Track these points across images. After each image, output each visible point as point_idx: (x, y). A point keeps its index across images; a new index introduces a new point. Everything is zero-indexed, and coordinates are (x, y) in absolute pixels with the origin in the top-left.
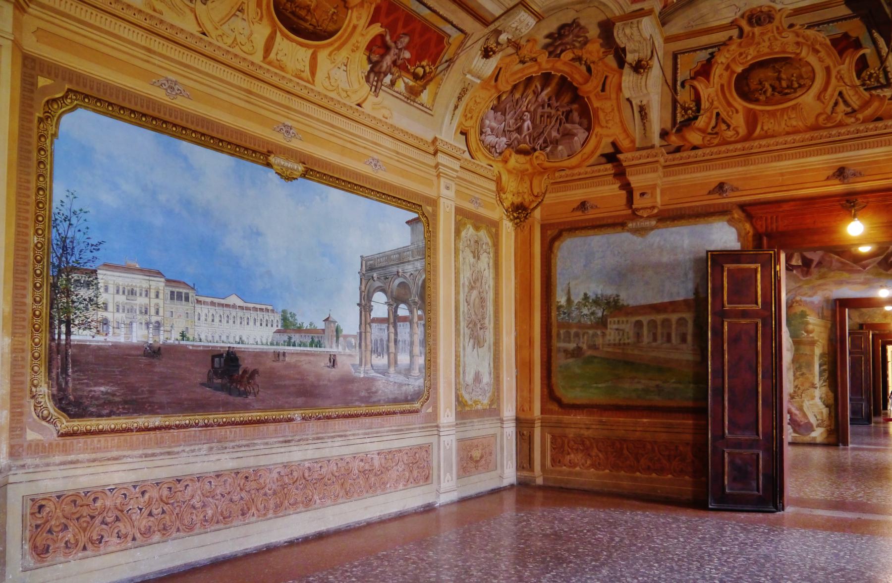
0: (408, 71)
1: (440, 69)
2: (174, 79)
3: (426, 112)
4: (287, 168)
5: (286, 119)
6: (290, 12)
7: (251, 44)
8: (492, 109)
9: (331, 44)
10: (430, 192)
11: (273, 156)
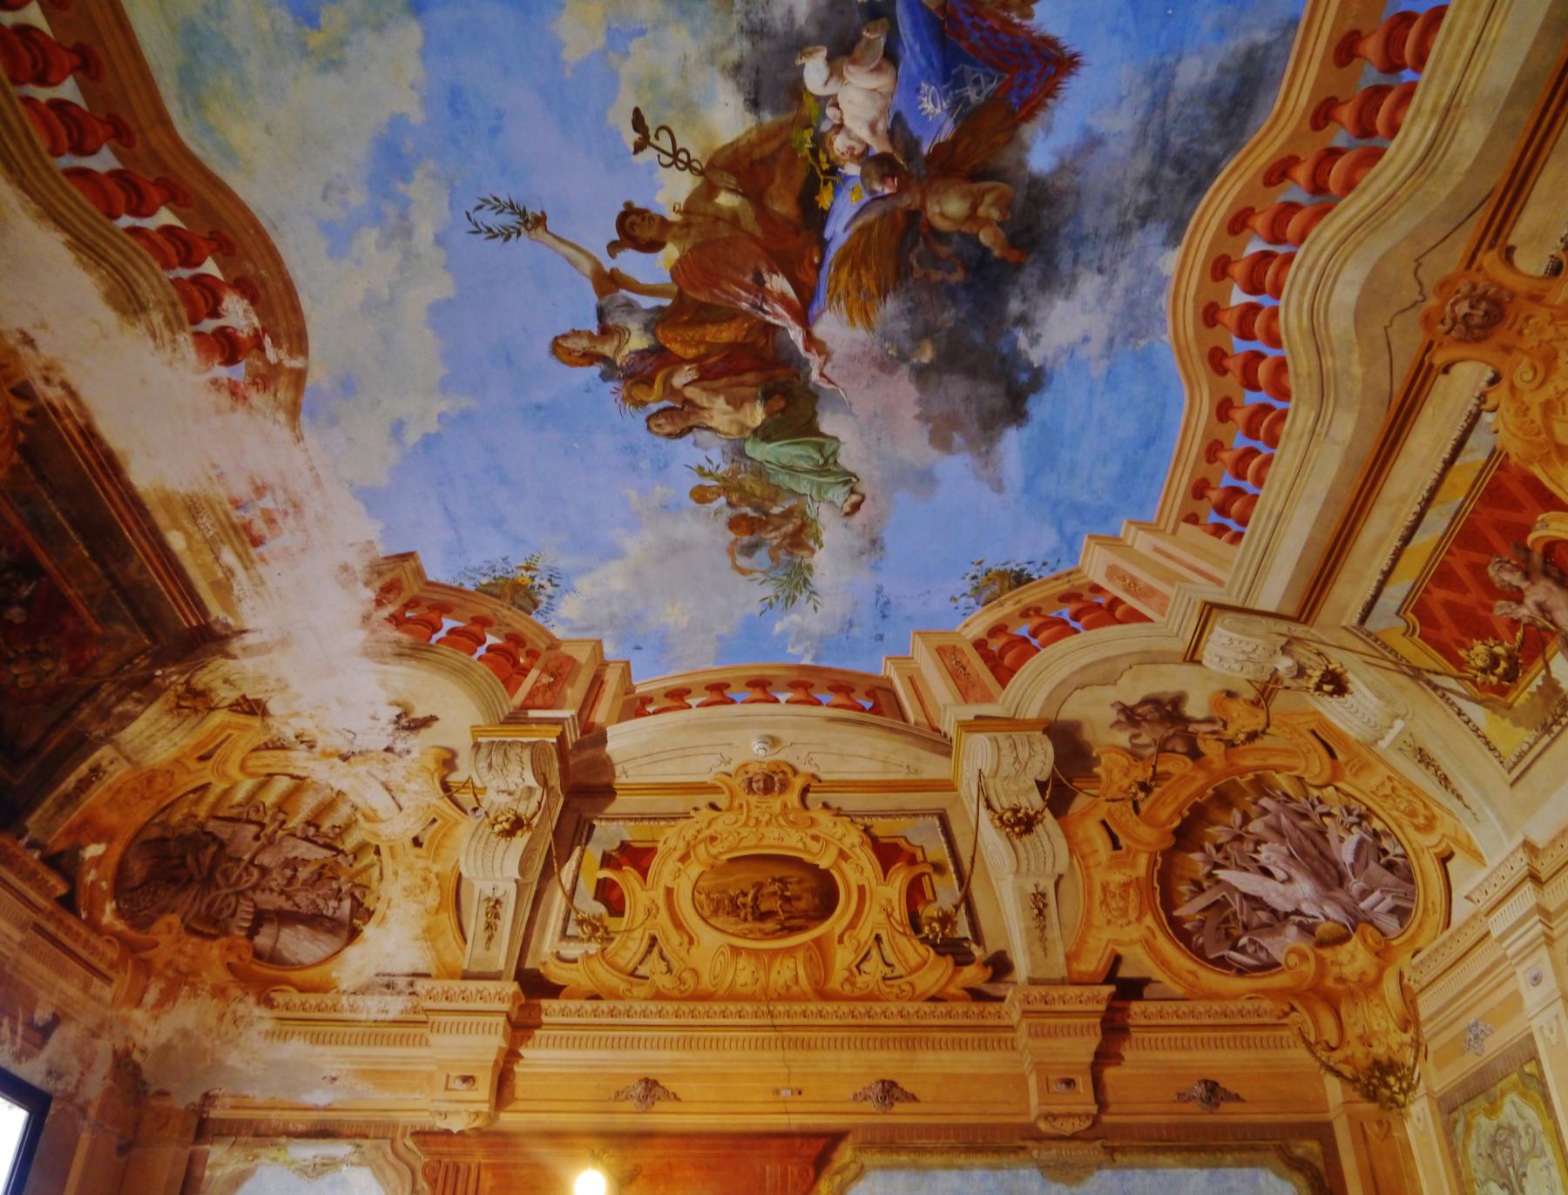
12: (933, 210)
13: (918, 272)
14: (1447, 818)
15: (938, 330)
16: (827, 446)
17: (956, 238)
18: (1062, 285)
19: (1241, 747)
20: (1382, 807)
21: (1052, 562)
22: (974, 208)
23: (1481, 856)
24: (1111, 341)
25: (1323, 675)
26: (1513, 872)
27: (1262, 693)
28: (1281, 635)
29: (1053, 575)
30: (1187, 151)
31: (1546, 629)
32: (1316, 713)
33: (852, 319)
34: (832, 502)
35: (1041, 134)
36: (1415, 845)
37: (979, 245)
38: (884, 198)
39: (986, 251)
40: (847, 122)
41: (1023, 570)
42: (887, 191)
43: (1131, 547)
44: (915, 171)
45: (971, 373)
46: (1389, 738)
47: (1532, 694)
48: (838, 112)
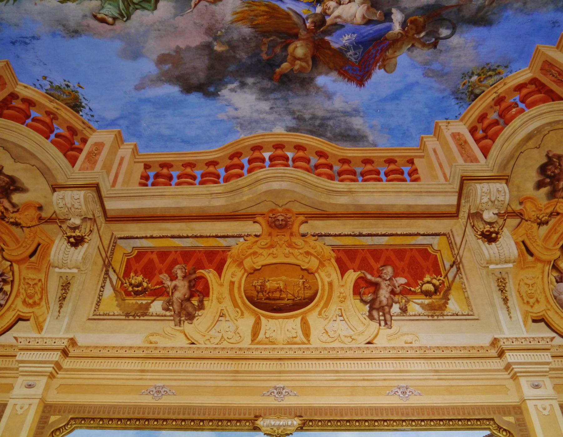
0: (414, 293)
1: (451, 276)
2: (162, 385)
3: (466, 320)
4: (279, 426)
5: (278, 382)
6: (265, 299)
7: (238, 335)
8: (557, 282)
9: (317, 305)
10: (511, 399)
11: (261, 419)
12: (298, 44)
13: (265, 40)
14: (44, 309)
15: (234, 52)
16: (150, 5)
17: (284, 54)
18: (263, 96)
19: (4, 222)
20: (19, 285)
21: (96, 118)
22: (299, 59)
23: (42, 329)
24: (238, 118)
25: (79, 236)
26: (53, 344)
27: (49, 219)
28: (94, 215)
29: (86, 121)
30: (327, 126)
31: (168, 293)
32: (53, 242)
33: (238, 13)
34: (103, 8)
35: (333, 79)
36: (13, 306)
37: (282, 63)
38: (305, 23)
39: (279, 66)
40: (341, 7)
41: (83, 107)
42: (308, 25)
43: (120, 148)
44: (317, 35)
45: (211, 68)
46: (63, 270)
47: (137, 303)
48: (347, 3)
